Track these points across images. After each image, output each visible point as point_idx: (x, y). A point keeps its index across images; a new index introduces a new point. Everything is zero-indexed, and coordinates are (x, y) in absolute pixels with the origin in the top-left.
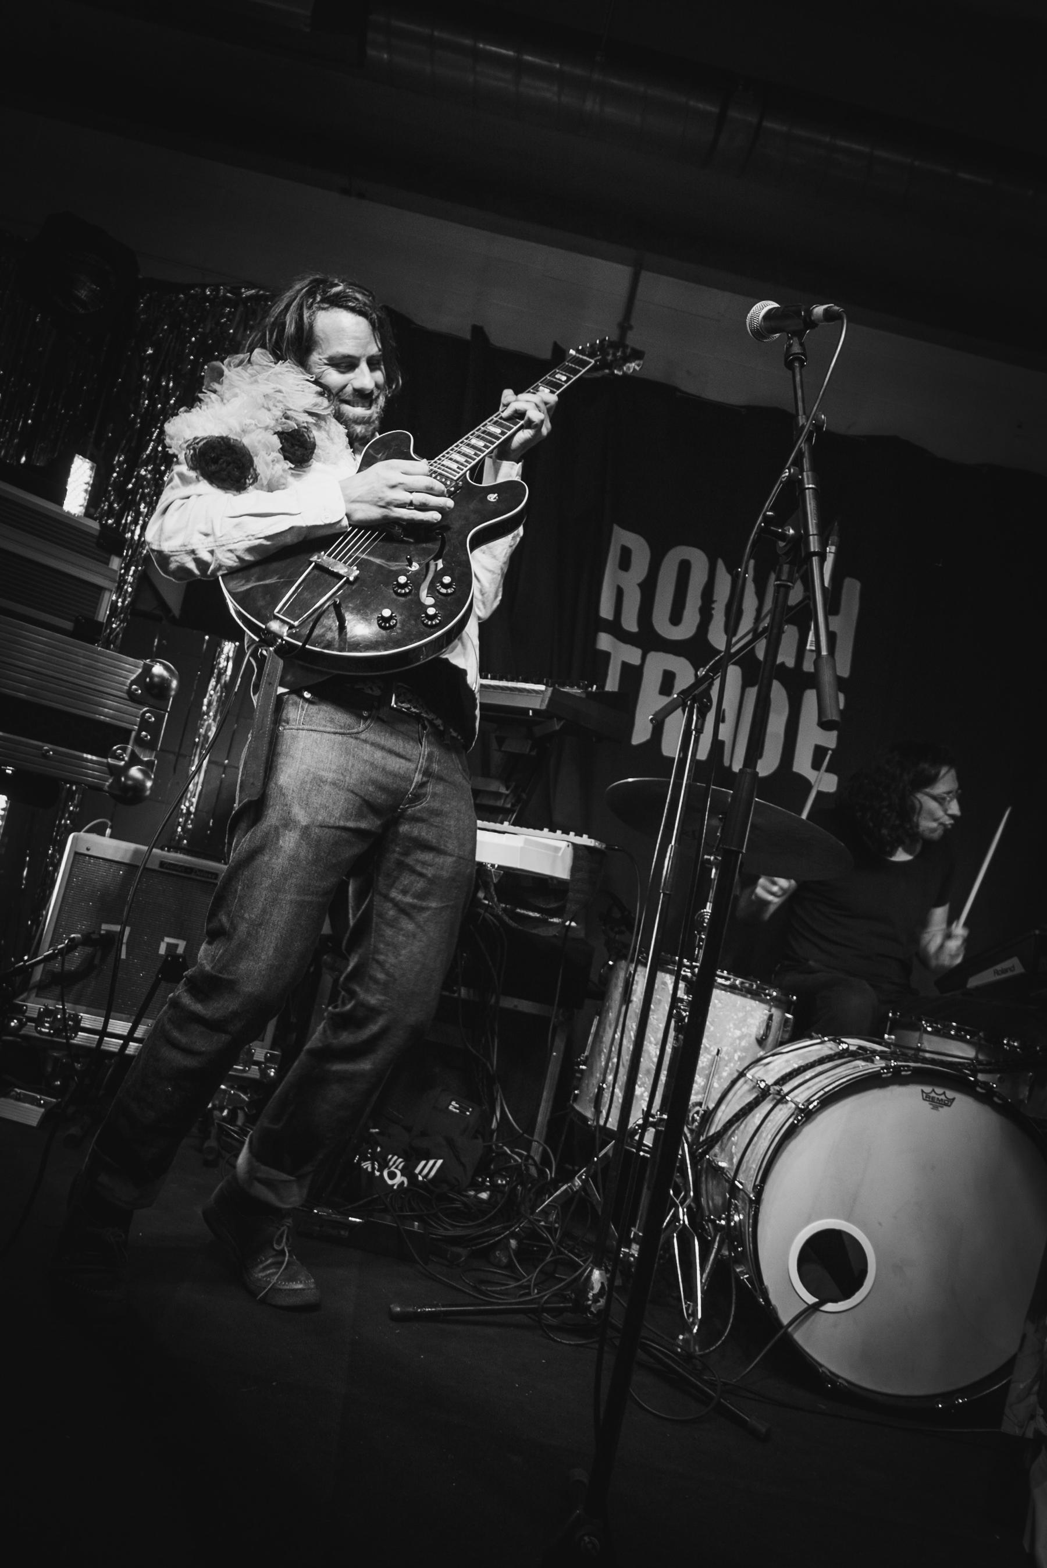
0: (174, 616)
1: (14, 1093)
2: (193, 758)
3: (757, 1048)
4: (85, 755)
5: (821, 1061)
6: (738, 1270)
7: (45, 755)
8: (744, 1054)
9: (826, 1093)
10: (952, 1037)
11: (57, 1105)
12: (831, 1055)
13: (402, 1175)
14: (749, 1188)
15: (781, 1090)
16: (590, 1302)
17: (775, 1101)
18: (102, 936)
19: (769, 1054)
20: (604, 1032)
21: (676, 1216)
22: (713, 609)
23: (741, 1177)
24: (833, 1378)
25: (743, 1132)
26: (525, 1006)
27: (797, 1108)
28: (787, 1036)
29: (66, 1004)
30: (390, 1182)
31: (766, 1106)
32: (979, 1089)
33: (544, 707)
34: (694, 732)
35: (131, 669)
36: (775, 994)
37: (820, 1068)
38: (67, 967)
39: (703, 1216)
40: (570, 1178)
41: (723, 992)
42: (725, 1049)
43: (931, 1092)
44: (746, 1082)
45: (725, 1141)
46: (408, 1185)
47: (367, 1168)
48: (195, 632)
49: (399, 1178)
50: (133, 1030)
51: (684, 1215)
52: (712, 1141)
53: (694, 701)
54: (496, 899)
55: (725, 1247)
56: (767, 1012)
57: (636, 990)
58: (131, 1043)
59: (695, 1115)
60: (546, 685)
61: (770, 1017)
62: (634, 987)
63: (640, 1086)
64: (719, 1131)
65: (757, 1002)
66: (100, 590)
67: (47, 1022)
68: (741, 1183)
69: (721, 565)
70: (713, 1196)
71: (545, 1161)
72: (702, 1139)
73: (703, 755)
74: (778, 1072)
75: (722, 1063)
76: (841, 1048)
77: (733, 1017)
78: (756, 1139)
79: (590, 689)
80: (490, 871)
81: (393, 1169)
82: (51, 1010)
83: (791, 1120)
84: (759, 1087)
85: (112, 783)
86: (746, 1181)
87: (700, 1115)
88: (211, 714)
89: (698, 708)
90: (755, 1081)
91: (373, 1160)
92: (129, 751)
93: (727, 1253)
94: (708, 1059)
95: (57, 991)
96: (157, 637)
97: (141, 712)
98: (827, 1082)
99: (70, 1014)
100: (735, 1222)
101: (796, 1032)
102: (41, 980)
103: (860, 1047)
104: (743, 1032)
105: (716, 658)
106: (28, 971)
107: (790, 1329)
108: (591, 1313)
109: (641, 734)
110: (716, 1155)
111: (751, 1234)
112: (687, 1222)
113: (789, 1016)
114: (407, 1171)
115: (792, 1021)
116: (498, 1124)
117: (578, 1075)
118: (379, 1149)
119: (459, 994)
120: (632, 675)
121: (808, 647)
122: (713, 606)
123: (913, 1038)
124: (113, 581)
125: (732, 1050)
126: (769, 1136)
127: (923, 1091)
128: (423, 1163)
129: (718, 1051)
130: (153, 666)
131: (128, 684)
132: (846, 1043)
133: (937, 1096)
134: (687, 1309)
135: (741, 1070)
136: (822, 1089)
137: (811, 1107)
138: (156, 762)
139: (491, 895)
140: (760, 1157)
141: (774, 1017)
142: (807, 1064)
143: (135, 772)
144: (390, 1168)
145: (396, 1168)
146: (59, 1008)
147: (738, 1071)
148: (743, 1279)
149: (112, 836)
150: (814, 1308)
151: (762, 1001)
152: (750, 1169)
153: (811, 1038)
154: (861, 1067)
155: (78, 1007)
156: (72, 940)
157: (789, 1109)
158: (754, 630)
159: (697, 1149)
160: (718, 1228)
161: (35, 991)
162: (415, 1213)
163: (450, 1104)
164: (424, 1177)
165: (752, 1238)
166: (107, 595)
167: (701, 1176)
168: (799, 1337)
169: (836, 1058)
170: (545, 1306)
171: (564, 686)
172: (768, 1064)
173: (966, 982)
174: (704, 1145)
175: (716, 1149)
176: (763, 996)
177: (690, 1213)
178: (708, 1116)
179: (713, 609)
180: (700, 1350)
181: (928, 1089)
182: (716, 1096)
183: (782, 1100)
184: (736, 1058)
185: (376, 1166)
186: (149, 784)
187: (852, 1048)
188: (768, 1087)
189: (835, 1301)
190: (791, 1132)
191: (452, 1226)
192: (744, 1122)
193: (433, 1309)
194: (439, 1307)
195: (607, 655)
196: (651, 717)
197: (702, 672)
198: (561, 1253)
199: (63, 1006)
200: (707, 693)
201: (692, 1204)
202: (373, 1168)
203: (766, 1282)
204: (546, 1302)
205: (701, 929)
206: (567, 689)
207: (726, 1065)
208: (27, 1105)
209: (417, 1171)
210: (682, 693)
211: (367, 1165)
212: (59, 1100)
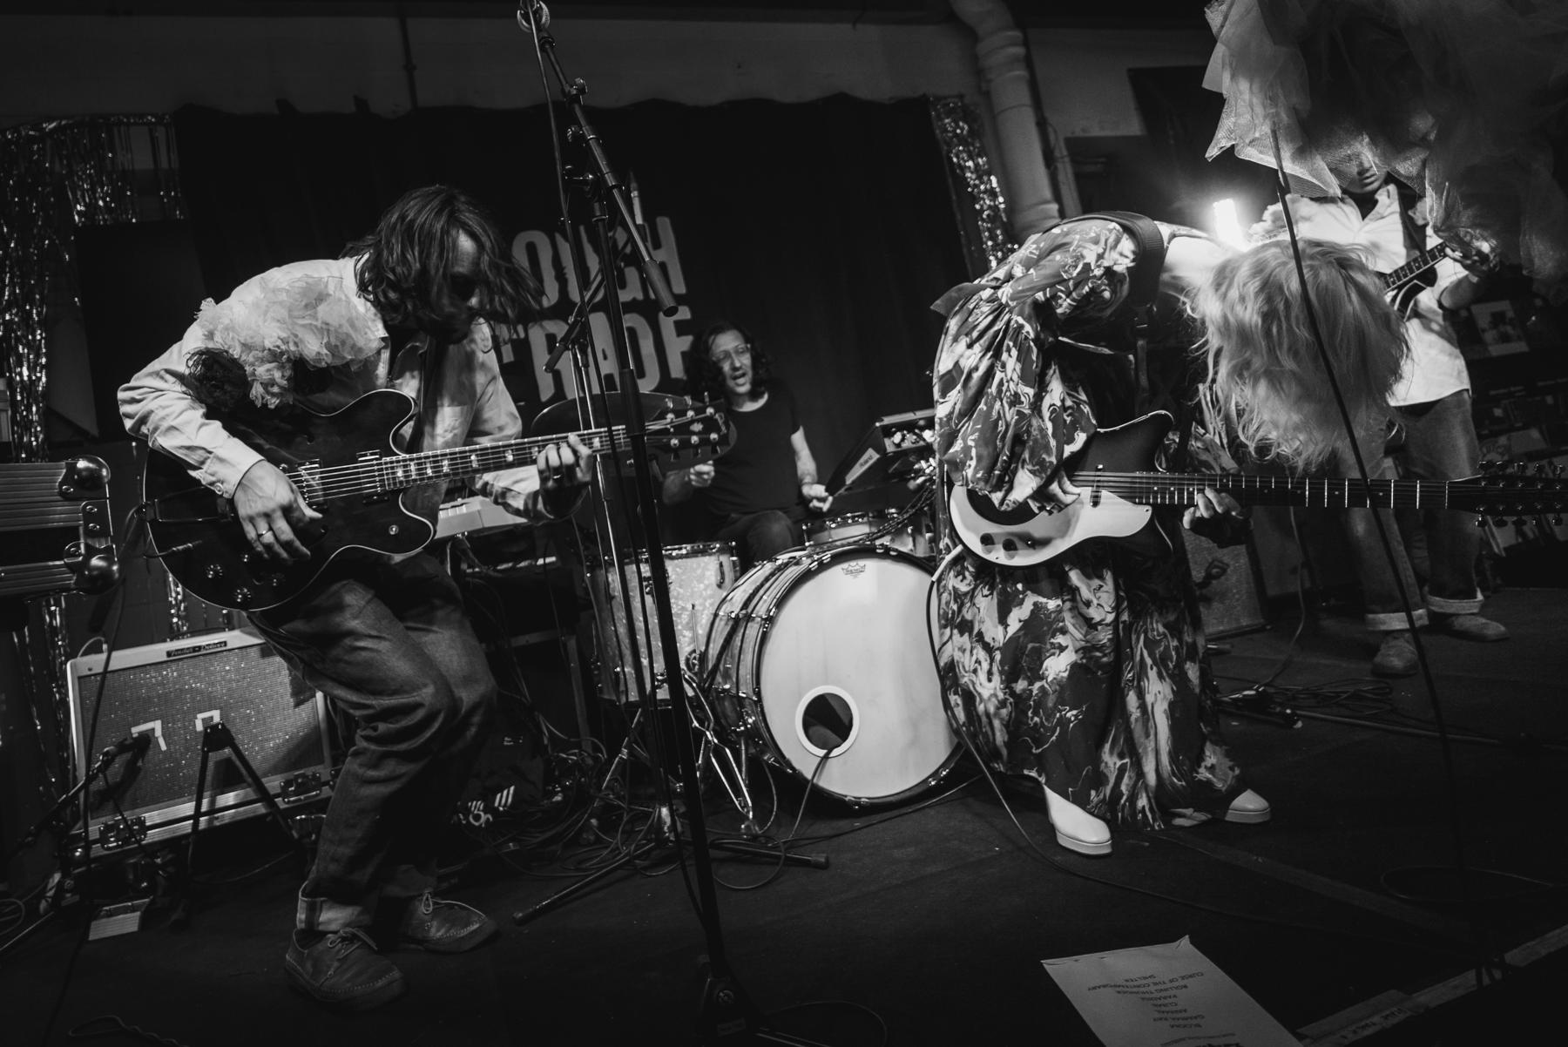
1: (102, 913)
3: (720, 591)
5: (767, 579)
6: (766, 758)
10: (850, 525)
13: (485, 813)
14: (751, 692)
21: (708, 742)
26: (533, 638)
27: (763, 619)
28: (738, 574)
32: (878, 551)
36: (718, 546)
42: (697, 603)
44: (721, 620)
49: (484, 817)
58: (202, 819)
61: (721, 565)
71: (597, 749)
75: (699, 614)
82: (112, 825)
93: (754, 751)
98: (776, 591)
99: (132, 820)
101: (744, 567)
113: (735, 558)
116: (549, 740)
117: (596, 672)
123: (824, 536)
128: (499, 796)
129: (693, 606)
134: (740, 804)
137: (771, 614)
150: (826, 757)
151: (710, 555)
153: (755, 566)
154: (793, 572)
155: (137, 810)
160: (739, 734)
173: (844, 482)
177: (716, 734)
178: (703, 657)
182: (704, 640)
184: (707, 604)
188: (737, 615)
190: (764, 639)
198: (632, 810)
201: (717, 728)
208: (121, 916)
209: (496, 804)
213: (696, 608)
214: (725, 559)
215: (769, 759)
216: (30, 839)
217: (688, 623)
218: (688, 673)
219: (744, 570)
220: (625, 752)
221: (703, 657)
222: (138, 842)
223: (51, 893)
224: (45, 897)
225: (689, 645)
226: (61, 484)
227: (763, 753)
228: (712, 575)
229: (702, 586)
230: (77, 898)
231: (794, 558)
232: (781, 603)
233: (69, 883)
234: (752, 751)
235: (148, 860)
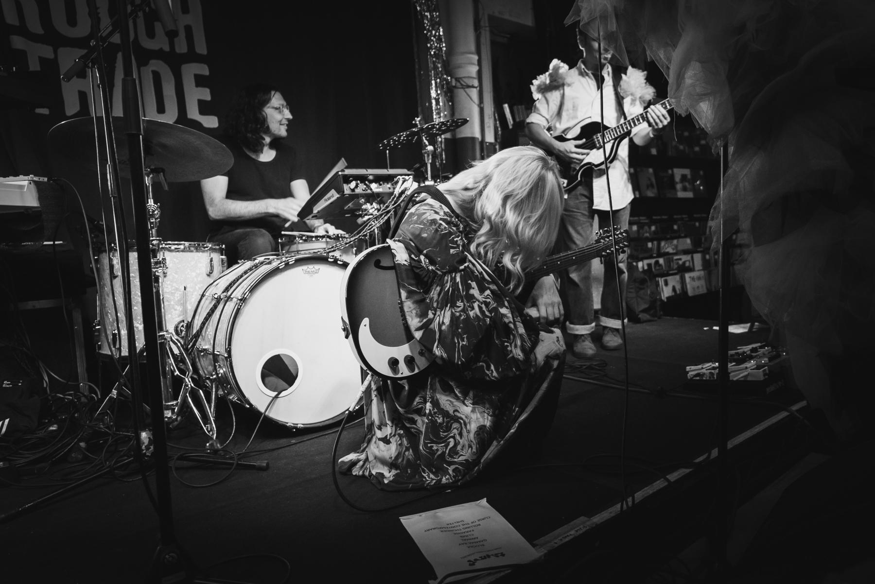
20: (105, 301)
36: (210, 246)
41: (177, 253)
45: (203, 334)
59: (182, 328)
61: (211, 260)
65: (201, 253)
86: (220, 349)
94: (180, 294)
100: (222, 374)
107: (267, 413)
111: (231, 376)
112: (192, 385)
123: (294, 248)
129: (185, 287)
135: (201, 293)
141: (213, 260)
147: (200, 295)
151: (203, 252)
153: (238, 263)
160: (212, 381)
165: (234, 379)
167: (195, 359)
172: (217, 285)
176: (203, 248)
178: (189, 326)
180: (221, 445)
184: (197, 288)
213: (187, 289)
215: (233, 398)
217: (179, 301)
218: (176, 337)
219: (229, 266)
221: (189, 326)
225: (179, 316)
227: (229, 394)
228: (204, 267)
229: (194, 274)
232: (253, 289)
234: (221, 392)
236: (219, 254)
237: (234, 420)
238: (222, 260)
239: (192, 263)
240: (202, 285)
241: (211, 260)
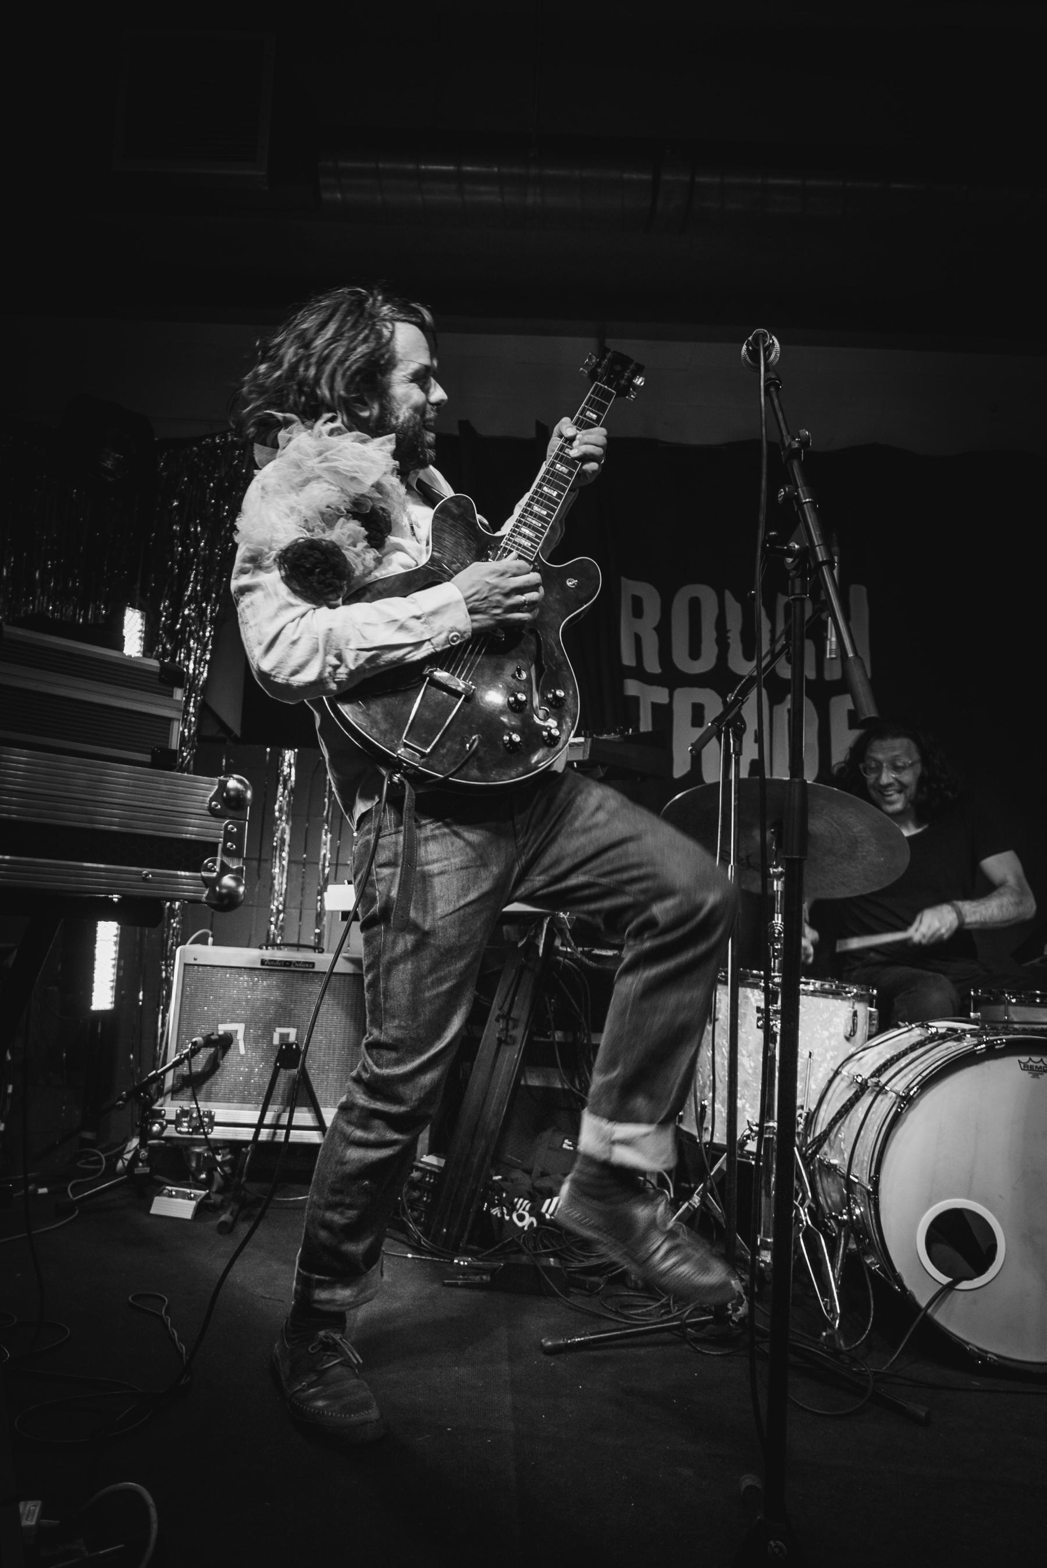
0: (236, 736)
2: (274, 860)
3: (847, 1044)
4: (179, 873)
5: (913, 1048)
6: (868, 1262)
7: (145, 879)
8: (836, 1053)
9: (924, 1078)
11: (207, 1196)
12: (921, 1040)
13: (531, 1216)
14: (865, 1180)
15: (879, 1081)
16: (730, 1312)
17: (875, 1093)
18: (220, 1036)
19: (859, 1050)
22: (729, 638)
23: (855, 1171)
24: (982, 1354)
25: (848, 1127)
27: (898, 1095)
28: (874, 1029)
29: (199, 1103)
30: (520, 1224)
31: (866, 1100)
33: (587, 757)
34: (733, 755)
35: (206, 789)
36: (855, 990)
37: (913, 1055)
38: (194, 1070)
39: (824, 1215)
40: (688, 1195)
42: (815, 1052)
43: (1028, 1062)
46: (538, 1224)
47: (497, 1214)
48: (257, 747)
49: (529, 1220)
50: (262, 1117)
51: (805, 1215)
52: (819, 1140)
53: (728, 726)
54: (573, 944)
55: (852, 1240)
56: (851, 1009)
57: (720, 1008)
58: (262, 1130)
60: (585, 736)
61: (855, 1014)
62: (717, 1006)
63: (741, 1099)
64: (825, 1131)
65: (839, 1001)
66: (169, 720)
67: (185, 1122)
68: (856, 1177)
69: (728, 594)
70: (831, 1192)
72: (809, 1140)
73: (744, 774)
74: (873, 1064)
75: (815, 1065)
76: (930, 1032)
77: (818, 1019)
78: (862, 1132)
79: (626, 733)
80: (563, 918)
81: (520, 1211)
83: (894, 1109)
84: (857, 1081)
85: (209, 893)
86: (861, 1174)
87: (803, 1117)
88: (284, 818)
89: (733, 733)
90: (851, 1076)
91: (501, 1204)
92: (218, 863)
93: (854, 1246)
95: (189, 1092)
96: (224, 757)
97: (224, 824)
100: (857, 1216)
102: (173, 1085)
103: (949, 1029)
104: (830, 1033)
105: (742, 682)
106: (159, 1079)
107: (929, 1311)
108: (733, 1322)
109: (680, 768)
110: (826, 1154)
112: (810, 1223)
113: (873, 1010)
114: (535, 1211)
115: (876, 1014)
118: (504, 1195)
119: (554, 1038)
120: (663, 714)
121: (828, 656)
122: (729, 635)
124: (179, 710)
125: (824, 1051)
126: (876, 1128)
127: (1019, 1062)
128: (548, 1201)
129: (810, 1053)
130: (227, 781)
131: (208, 802)
132: (934, 1027)
133: (1035, 1065)
135: (836, 1069)
136: (920, 1075)
137: (912, 1093)
138: (244, 868)
139: (568, 940)
140: (870, 1149)
141: (858, 1013)
142: (900, 1053)
143: (227, 881)
144: (518, 1211)
145: (524, 1210)
146: (193, 1108)
147: (832, 1070)
148: (875, 1270)
149: (214, 944)
150: (949, 1288)
151: (843, 999)
152: (863, 1161)
153: (899, 1027)
154: (951, 1048)
155: (210, 1104)
156: (194, 1044)
157: (891, 1098)
158: (771, 652)
159: (807, 1151)
160: (841, 1224)
161: (170, 1094)
162: (550, 1250)
163: (563, 1143)
164: (551, 1215)
166: (176, 724)
167: (815, 1176)
168: (940, 1317)
169: (927, 1042)
170: (688, 1321)
171: (601, 734)
172: (861, 1058)
174: (813, 1146)
175: (826, 1148)
176: (844, 994)
177: (811, 1213)
178: (811, 1118)
179: (729, 638)
181: (1024, 1059)
183: (881, 1090)
184: (829, 1057)
185: (505, 1211)
186: (241, 889)
187: (941, 1031)
189: (970, 1278)
190: (895, 1121)
191: (584, 1256)
192: (848, 1118)
193: (582, 1339)
194: (587, 1335)
195: (636, 700)
196: (690, 748)
197: (730, 698)
199: (197, 1104)
200: (739, 717)
201: (813, 1205)
202: (502, 1213)
203: (898, 1270)
204: (688, 1317)
205: (773, 940)
206: (605, 737)
207: (820, 1066)
209: (544, 1210)
210: (717, 720)
211: (495, 1211)
212: (207, 1191)
214: (863, 1009)
216: (121, 1102)
220: (696, 1200)
222: (205, 1134)
223: (128, 1156)
224: (122, 1158)
226: (212, 800)
227: (867, 1254)
229: (826, 1034)
230: (147, 1170)
231: (954, 1030)
233: (144, 1153)
235: (211, 1154)
236: (867, 1004)
237: (872, 1306)
238: (871, 1014)
239: (826, 1015)
240: (836, 1053)
241: (855, 1014)
